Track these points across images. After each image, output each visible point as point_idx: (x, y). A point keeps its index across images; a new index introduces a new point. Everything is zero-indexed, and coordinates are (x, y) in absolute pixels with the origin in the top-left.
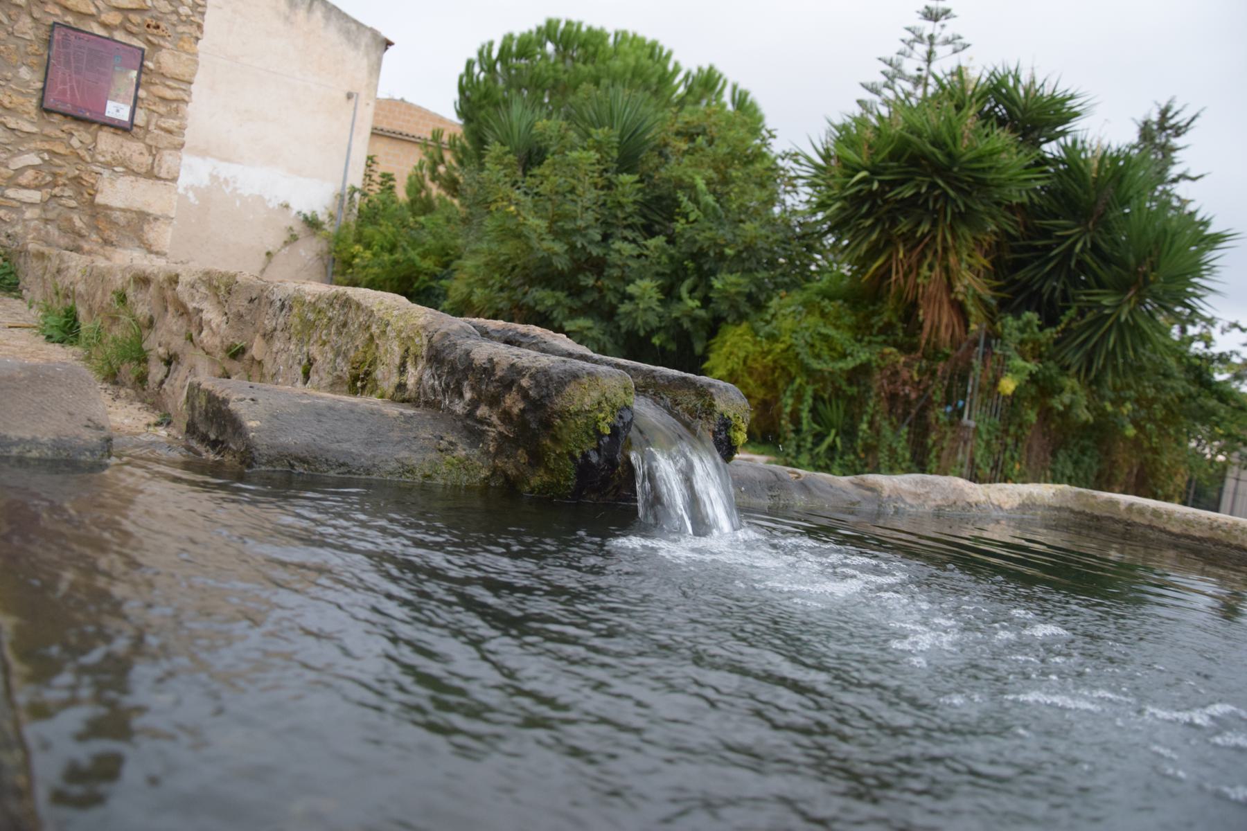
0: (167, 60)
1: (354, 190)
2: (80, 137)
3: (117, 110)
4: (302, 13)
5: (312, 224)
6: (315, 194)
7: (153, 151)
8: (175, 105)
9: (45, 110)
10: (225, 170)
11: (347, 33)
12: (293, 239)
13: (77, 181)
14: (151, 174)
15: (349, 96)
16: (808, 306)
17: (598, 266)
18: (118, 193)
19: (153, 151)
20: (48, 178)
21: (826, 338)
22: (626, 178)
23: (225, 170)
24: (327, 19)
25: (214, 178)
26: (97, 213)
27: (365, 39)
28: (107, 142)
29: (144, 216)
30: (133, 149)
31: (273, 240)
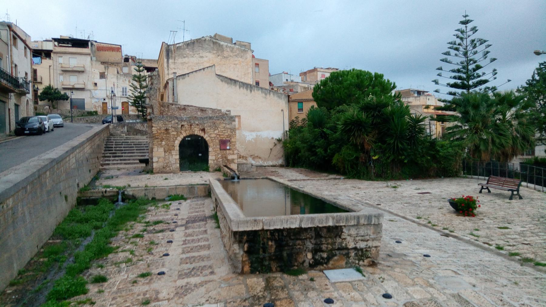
0: (233, 140)
1: (286, 131)
2: (225, 152)
3: (228, 148)
4: (268, 95)
5: (279, 140)
6: (278, 134)
7: (233, 151)
8: (234, 145)
9: (220, 150)
10: (259, 133)
11: (279, 97)
12: (275, 145)
13: (225, 157)
14: (233, 154)
15: (282, 110)
16: (347, 148)
17: (314, 146)
18: (230, 157)
19: (233, 151)
20: (222, 157)
21: (350, 153)
22: (316, 130)
23: (259, 133)
24: (274, 95)
25: (257, 136)
26: (228, 160)
27: (283, 96)
28: (228, 151)
29: (233, 160)
30: (231, 152)
31: (271, 146)
